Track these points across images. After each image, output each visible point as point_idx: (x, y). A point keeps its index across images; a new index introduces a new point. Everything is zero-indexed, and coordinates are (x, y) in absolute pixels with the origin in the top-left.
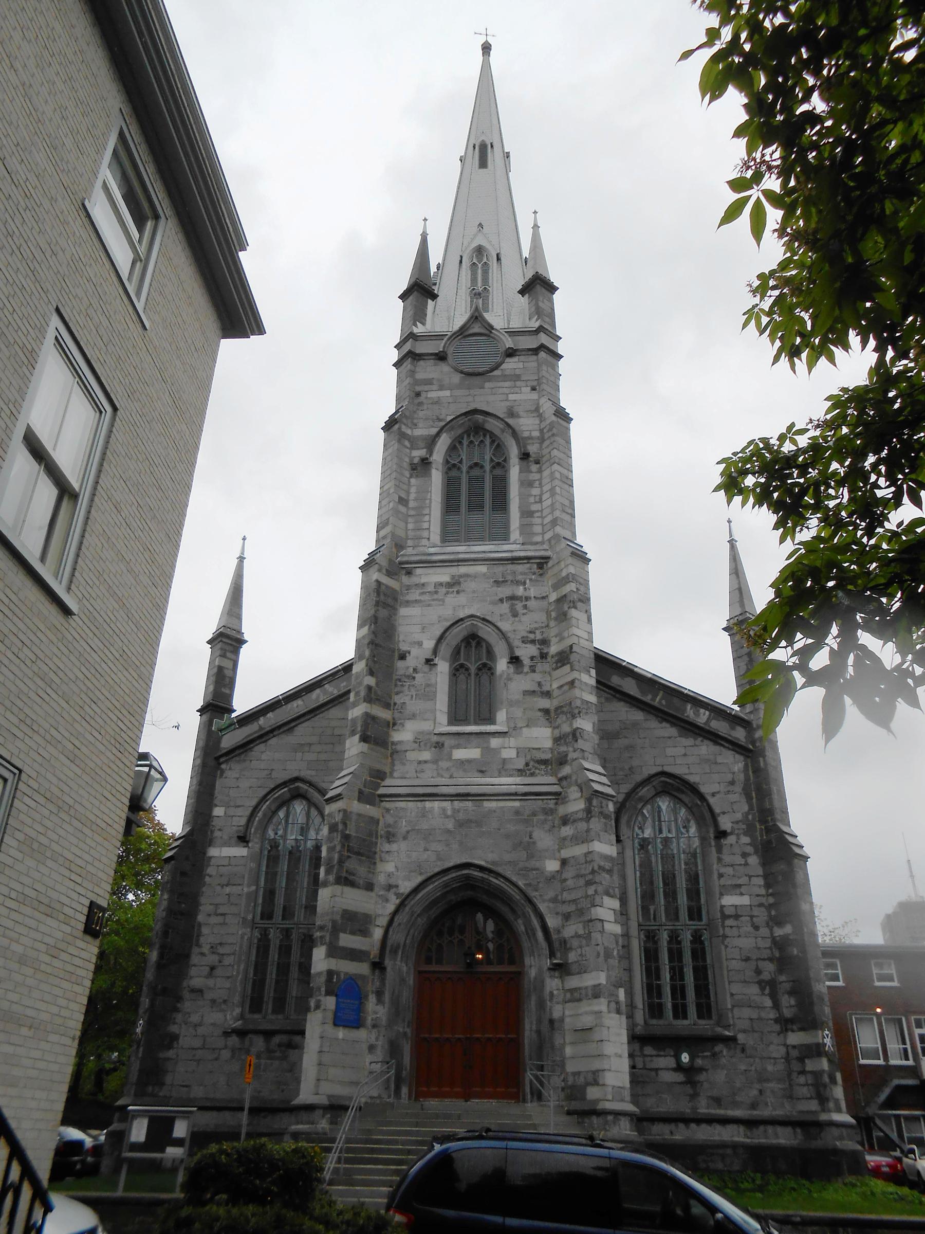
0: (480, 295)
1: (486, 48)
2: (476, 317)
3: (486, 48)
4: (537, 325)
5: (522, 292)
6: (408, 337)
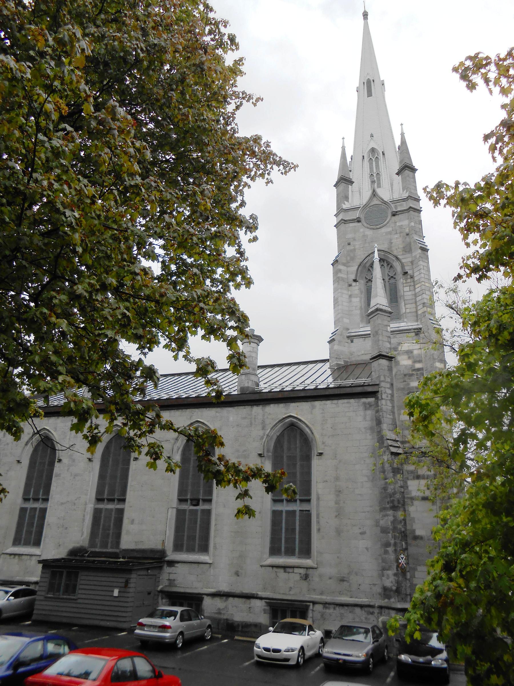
0: (375, 179)
1: (365, 15)
2: (374, 194)
3: (365, 15)
4: (407, 195)
5: (398, 174)
6: (340, 210)
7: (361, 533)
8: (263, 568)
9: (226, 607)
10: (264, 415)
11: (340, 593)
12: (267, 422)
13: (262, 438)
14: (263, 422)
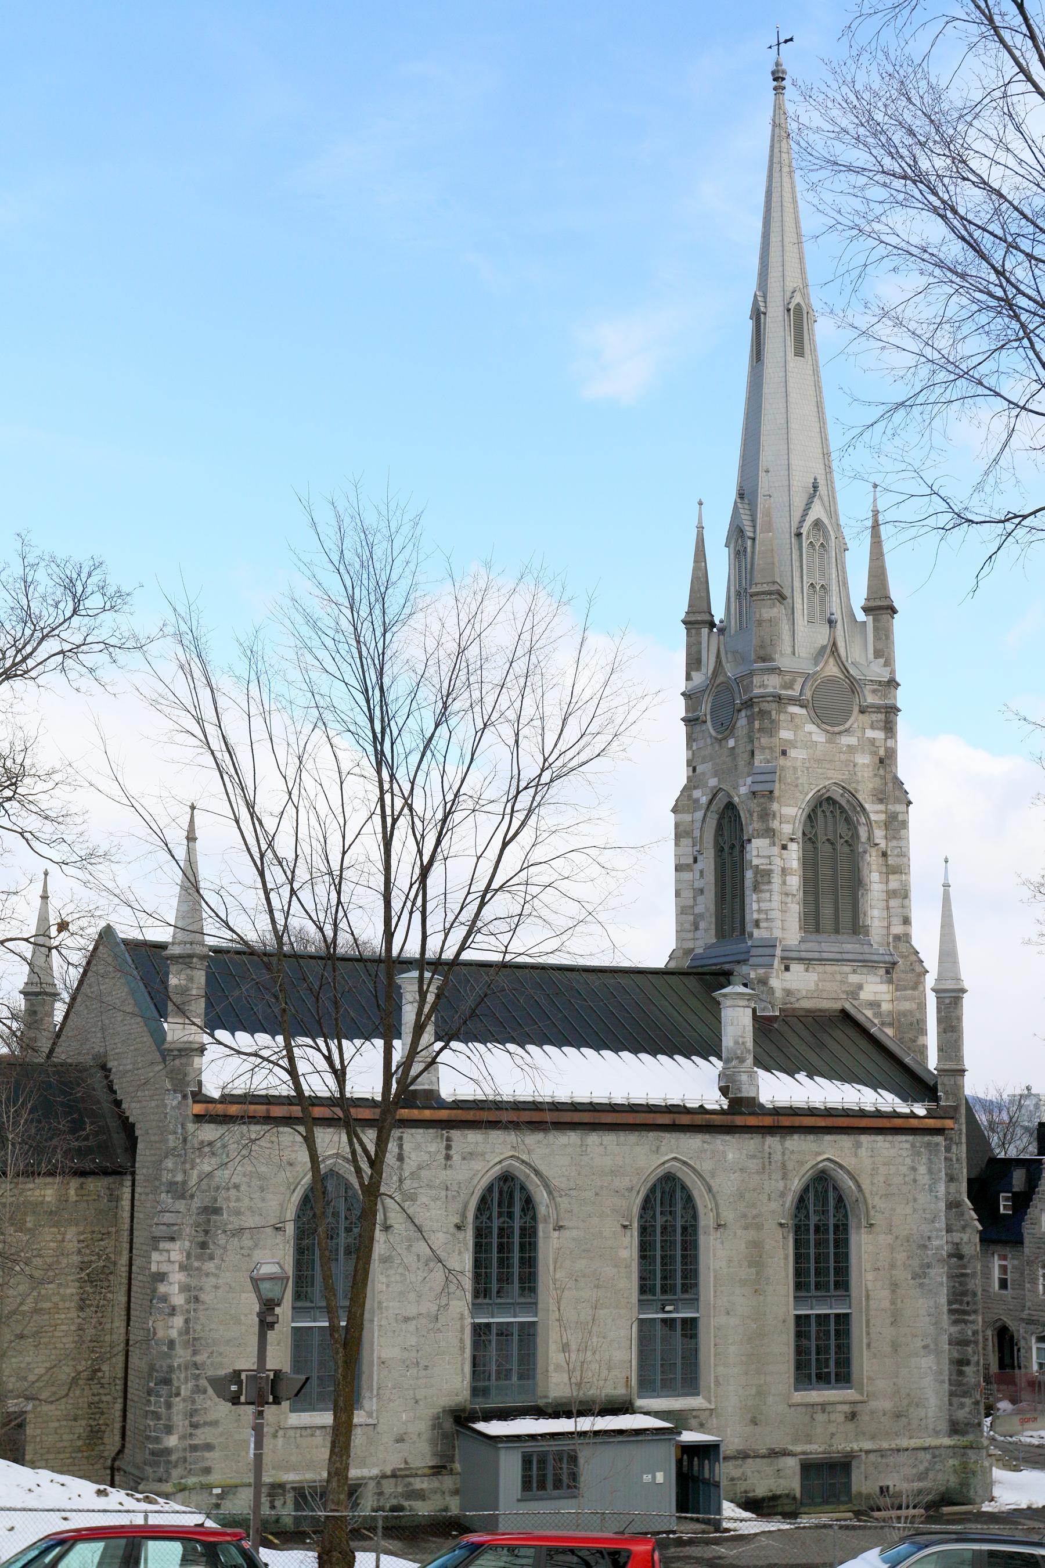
7: (925, 1347)
8: (793, 1409)
9: (743, 1473)
10: (783, 1154)
11: (897, 1434)
12: (790, 1165)
13: (782, 1195)
14: (784, 1165)
